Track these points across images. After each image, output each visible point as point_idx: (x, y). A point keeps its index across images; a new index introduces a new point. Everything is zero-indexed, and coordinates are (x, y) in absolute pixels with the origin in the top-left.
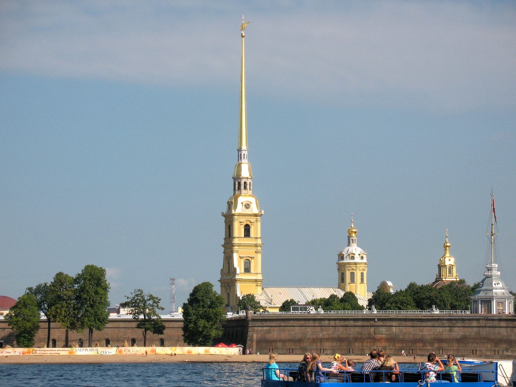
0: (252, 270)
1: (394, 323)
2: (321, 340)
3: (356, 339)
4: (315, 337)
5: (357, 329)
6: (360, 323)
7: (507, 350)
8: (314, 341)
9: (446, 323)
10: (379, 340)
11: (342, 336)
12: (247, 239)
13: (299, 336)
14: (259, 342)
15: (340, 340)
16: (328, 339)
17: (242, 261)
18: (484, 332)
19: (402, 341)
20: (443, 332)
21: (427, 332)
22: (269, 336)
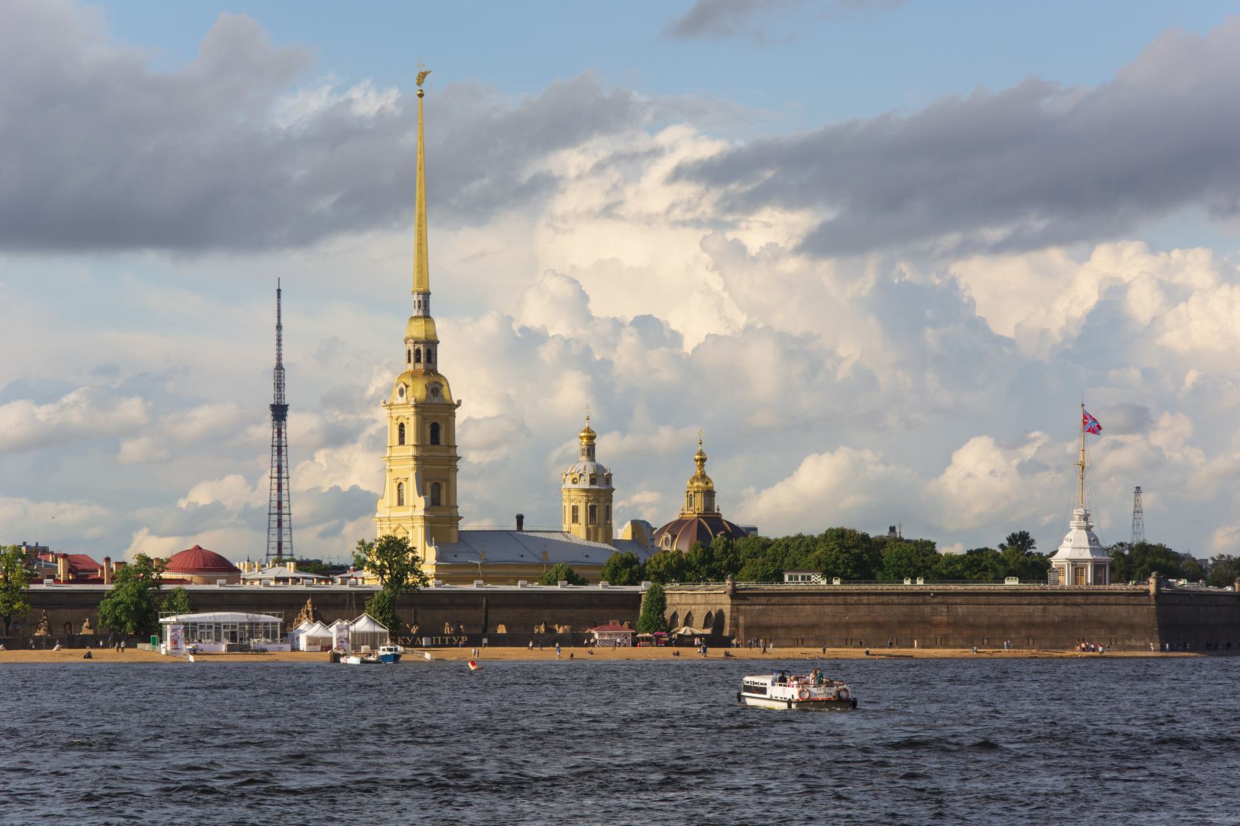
0: (443, 502)
1: (959, 600)
2: (847, 626)
3: (902, 624)
4: (837, 620)
5: (904, 609)
6: (908, 599)
7: (1129, 638)
8: (835, 626)
9: (1038, 599)
10: (936, 625)
11: (881, 619)
12: (436, 447)
13: (814, 619)
14: (748, 628)
15: (877, 625)
16: (859, 624)
17: (428, 485)
18: (1094, 611)
19: (971, 626)
20: (1035, 611)
21: (1012, 612)
22: (764, 620)
